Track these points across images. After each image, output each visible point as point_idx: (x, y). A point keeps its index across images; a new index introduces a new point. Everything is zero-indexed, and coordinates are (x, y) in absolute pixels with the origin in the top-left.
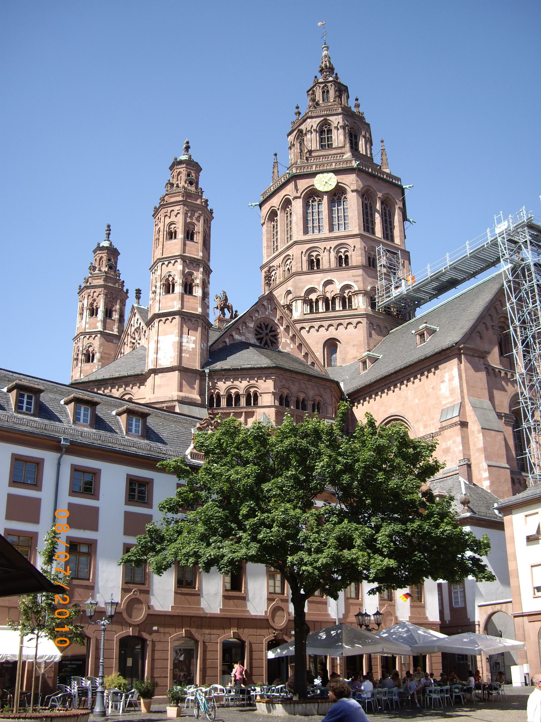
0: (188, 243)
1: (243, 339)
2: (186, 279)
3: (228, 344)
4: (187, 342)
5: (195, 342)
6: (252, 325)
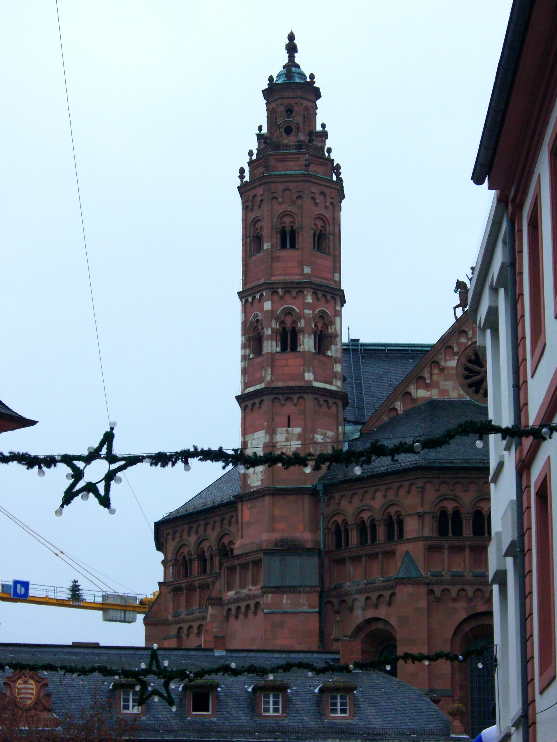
0: (284, 253)
1: (434, 394)
2: (282, 322)
3: (400, 412)
4: (287, 440)
5: (299, 437)
6: (453, 363)
